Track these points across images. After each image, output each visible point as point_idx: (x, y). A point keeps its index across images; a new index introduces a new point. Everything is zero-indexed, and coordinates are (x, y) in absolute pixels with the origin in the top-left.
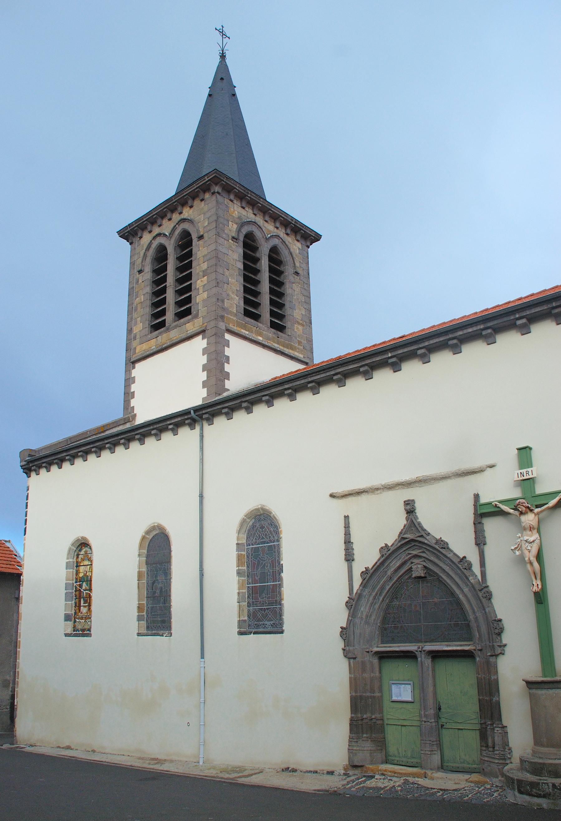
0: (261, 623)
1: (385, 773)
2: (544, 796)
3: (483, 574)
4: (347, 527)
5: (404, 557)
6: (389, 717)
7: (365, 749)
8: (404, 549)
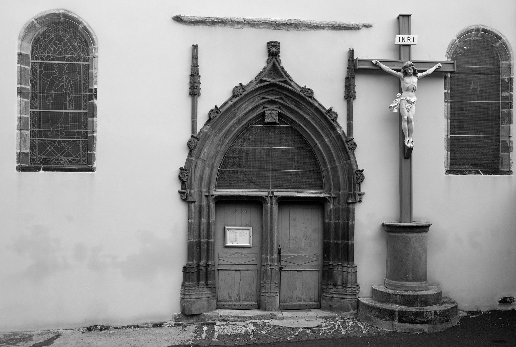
0: (52, 158)
1: (226, 318)
2: (427, 323)
3: (350, 127)
4: (195, 58)
5: (257, 101)
6: (220, 262)
7: (203, 296)
8: (261, 92)
